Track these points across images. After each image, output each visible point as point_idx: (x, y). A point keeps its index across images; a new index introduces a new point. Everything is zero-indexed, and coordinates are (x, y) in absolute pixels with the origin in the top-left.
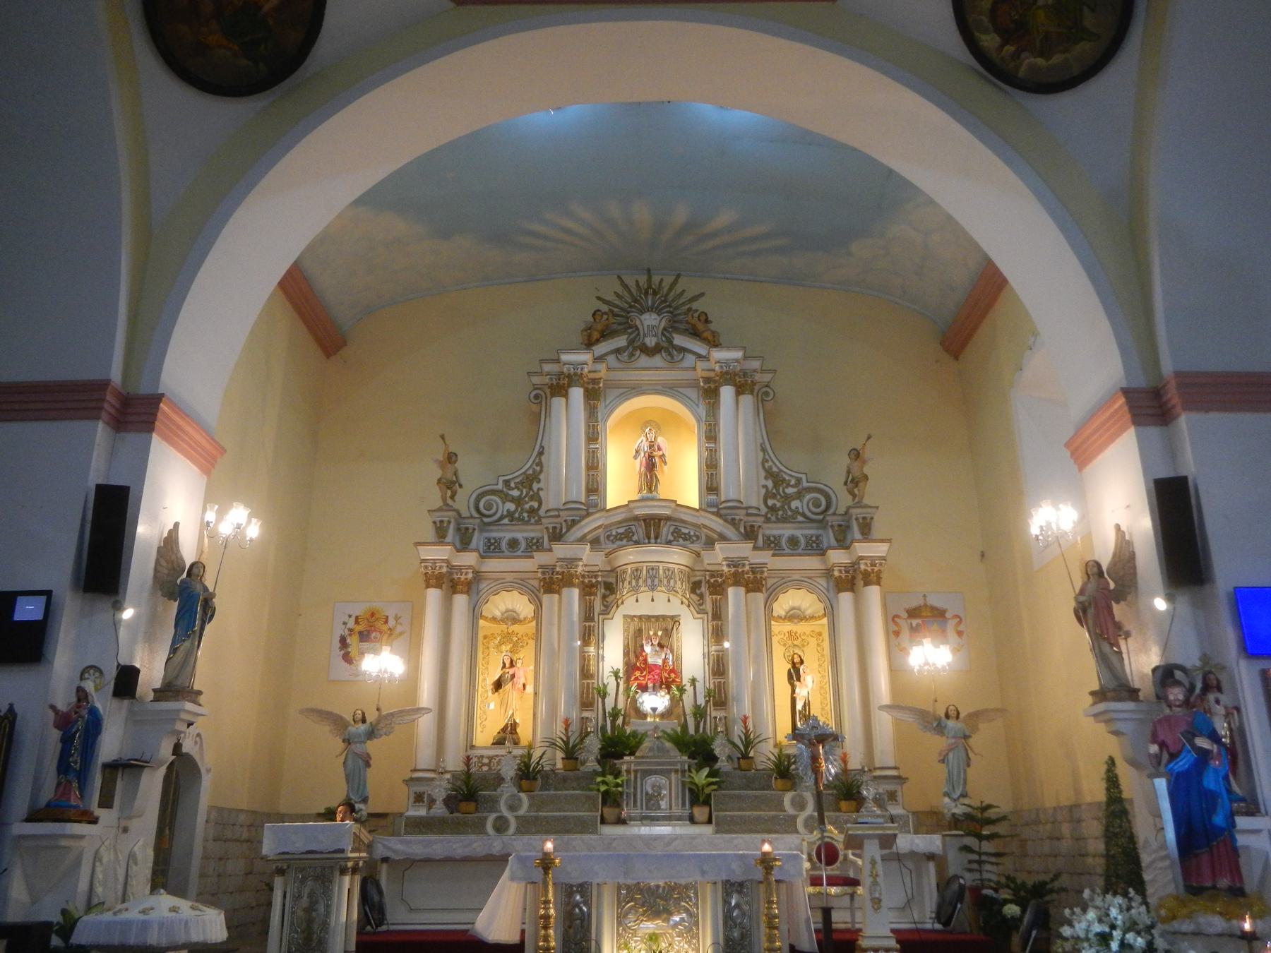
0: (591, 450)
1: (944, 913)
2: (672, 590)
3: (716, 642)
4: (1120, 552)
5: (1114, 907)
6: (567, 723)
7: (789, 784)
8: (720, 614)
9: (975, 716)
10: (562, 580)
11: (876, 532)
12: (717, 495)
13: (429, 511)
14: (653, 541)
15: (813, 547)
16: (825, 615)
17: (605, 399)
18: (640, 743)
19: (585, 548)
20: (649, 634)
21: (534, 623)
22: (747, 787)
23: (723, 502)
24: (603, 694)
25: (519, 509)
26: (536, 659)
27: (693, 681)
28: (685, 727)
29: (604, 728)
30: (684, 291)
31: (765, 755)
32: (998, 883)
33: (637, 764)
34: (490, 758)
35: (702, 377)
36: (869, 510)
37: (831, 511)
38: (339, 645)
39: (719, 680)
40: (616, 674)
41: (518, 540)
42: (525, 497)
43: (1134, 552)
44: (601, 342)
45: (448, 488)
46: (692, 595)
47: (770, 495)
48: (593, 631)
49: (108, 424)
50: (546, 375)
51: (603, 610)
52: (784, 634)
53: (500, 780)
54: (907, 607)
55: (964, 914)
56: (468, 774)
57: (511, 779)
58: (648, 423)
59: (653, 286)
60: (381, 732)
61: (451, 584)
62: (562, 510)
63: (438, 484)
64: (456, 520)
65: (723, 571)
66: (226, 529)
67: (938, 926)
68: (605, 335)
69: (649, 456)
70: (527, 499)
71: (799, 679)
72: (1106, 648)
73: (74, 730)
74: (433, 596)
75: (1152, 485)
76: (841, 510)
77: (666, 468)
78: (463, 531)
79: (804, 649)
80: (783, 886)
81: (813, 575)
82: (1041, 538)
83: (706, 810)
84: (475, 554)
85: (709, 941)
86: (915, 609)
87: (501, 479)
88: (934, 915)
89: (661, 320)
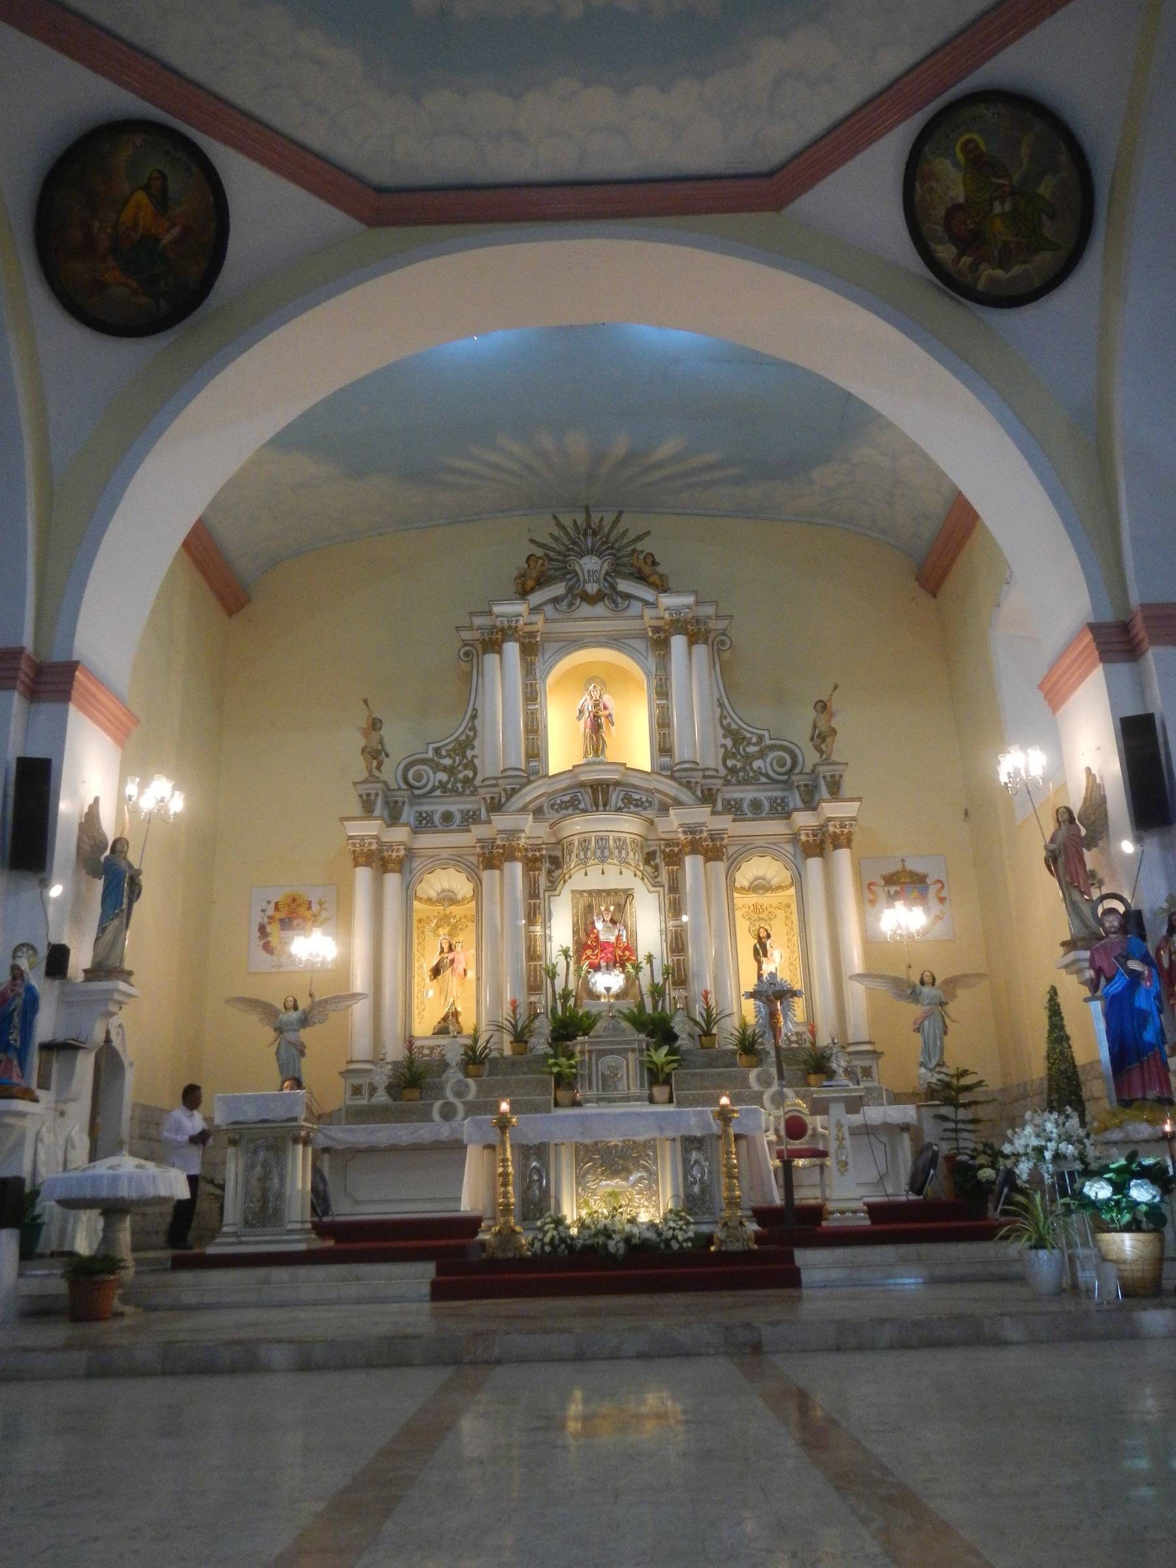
0: (529, 712)
1: (916, 1186)
2: (624, 862)
3: (673, 917)
4: (1091, 797)
5: (1050, 1122)
6: (515, 1006)
7: (754, 1059)
8: (678, 887)
9: (952, 983)
10: (503, 854)
11: (847, 789)
12: (671, 756)
13: (355, 783)
14: (601, 808)
15: (777, 810)
16: (792, 884)
17: (544, 655)
18: (592, 1025)
19: (527, 819)
20: (600, 909)
21: (474, 902)
22: (709, 1065)
23: (678, 764)
24: (553, 975)
25: (452, 779)
26: (477, 941)
27: (650, 958)
28: (641, 1006)
29: (554, 1009)
30: (626, 531)
31: (727, 1034)
32: (975, 1150)
33: (591, 1043)
34: (432, 1049)
35: (650, 626)
36: (835, 767)
37: (797, 771)
38: (259, 934)
39: (678, 958)
40: (565, 953)
41: (452, 813)
42: (458, 766)
43: (1105, 797)
44: (537, 590)
45: (374, 758)
46: (646, 867)
47: (730, 754)
48: (539, 909)
49: (23, 694)
50: (477, 630)
51: (549, 887)
52: (749, 908)
53: (444, 1065)
54: (884, 873)
55: (938, 1186)
56: (411, 1061)
57: (457, 1064)
58: (592, 679)
59: (593, 526)
60: (316, 1020)
61: (381, 863)
62: (500, 778)
63: (362, 754)
64: (383, 792)
65: (679, 838)
66: (147, 803)
67: (913, 1197)
68: (542, 582)
69: (594, 716)
70: (460, 768)
71: (765, 955)
72: (1076, 896)
73: (11, 1009)
74: (363, 876)
75: (1119, 725)
76: (808, 769)
77: (613, 729)
79: (771, 923)
80: (743, 1143)
81: (779, 841)
82: (1010, 785)
83: (666, 1089)
84: (407, 829)
85: (669, 1194)
86: (893, 875)
87: (431, 746)
88: (907, 1188)
89: (604, 562)
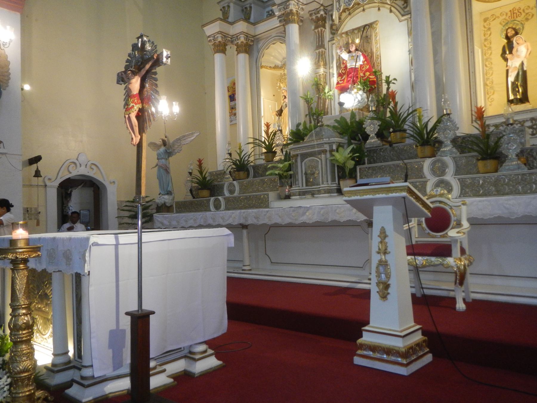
13: (219, 3)
51: (332, 38)
52: (507, 14)
60: (176, 151)
71: (511, 52)
78: (245, 11)
